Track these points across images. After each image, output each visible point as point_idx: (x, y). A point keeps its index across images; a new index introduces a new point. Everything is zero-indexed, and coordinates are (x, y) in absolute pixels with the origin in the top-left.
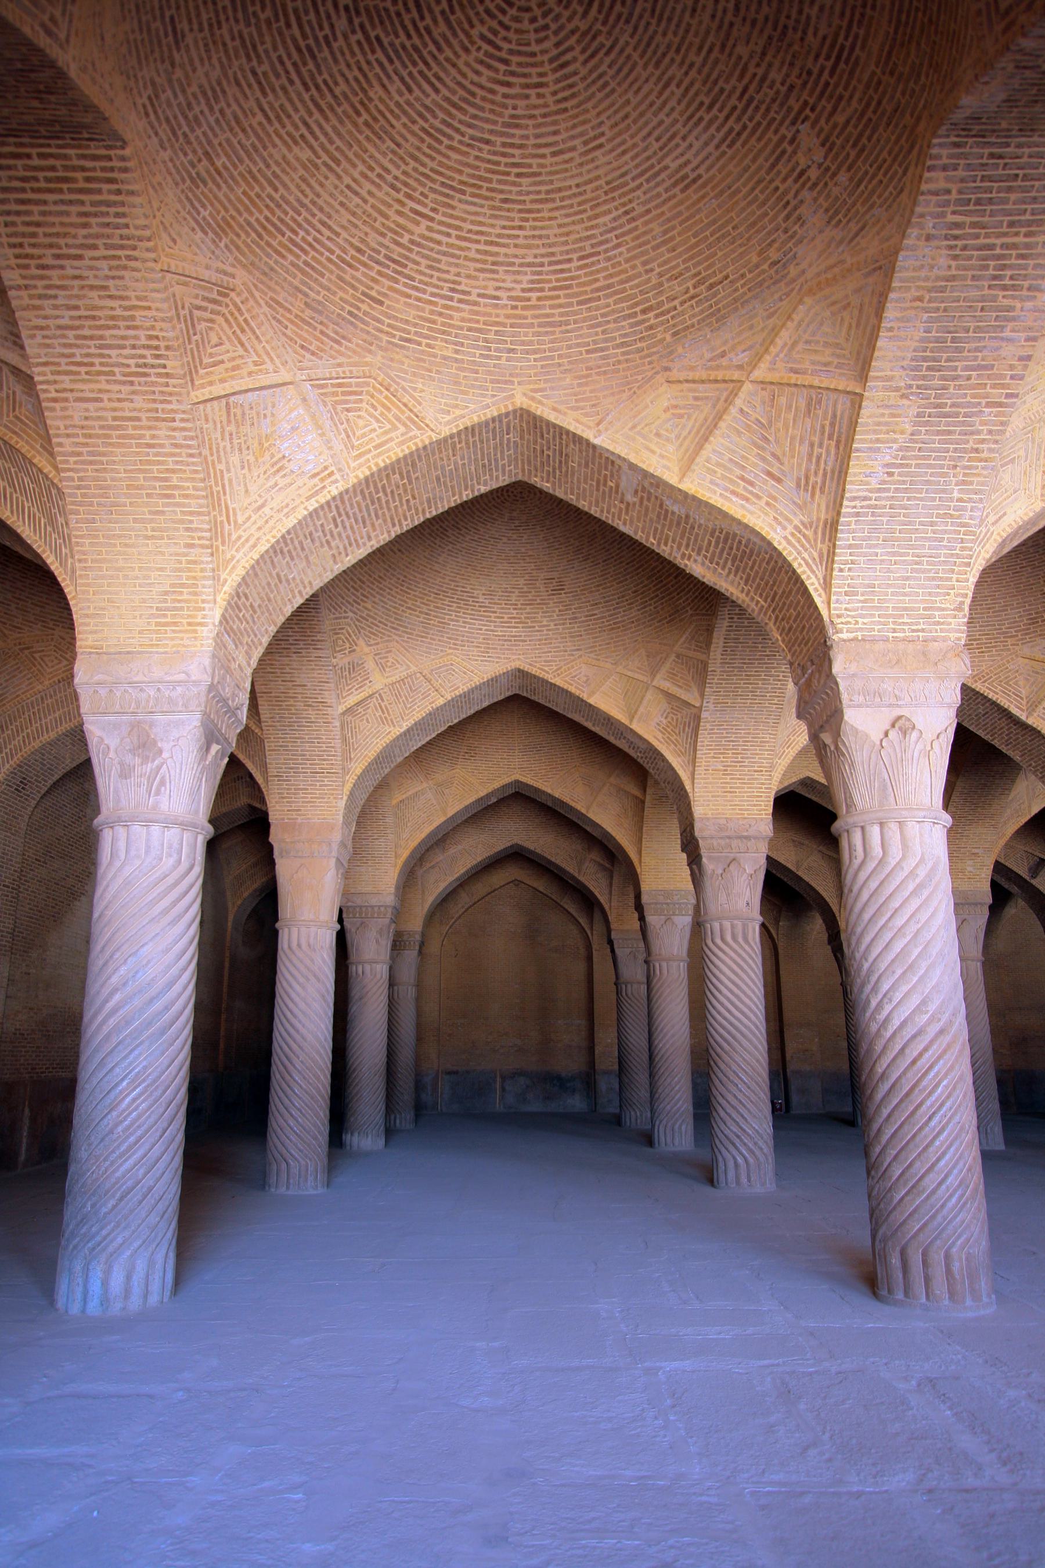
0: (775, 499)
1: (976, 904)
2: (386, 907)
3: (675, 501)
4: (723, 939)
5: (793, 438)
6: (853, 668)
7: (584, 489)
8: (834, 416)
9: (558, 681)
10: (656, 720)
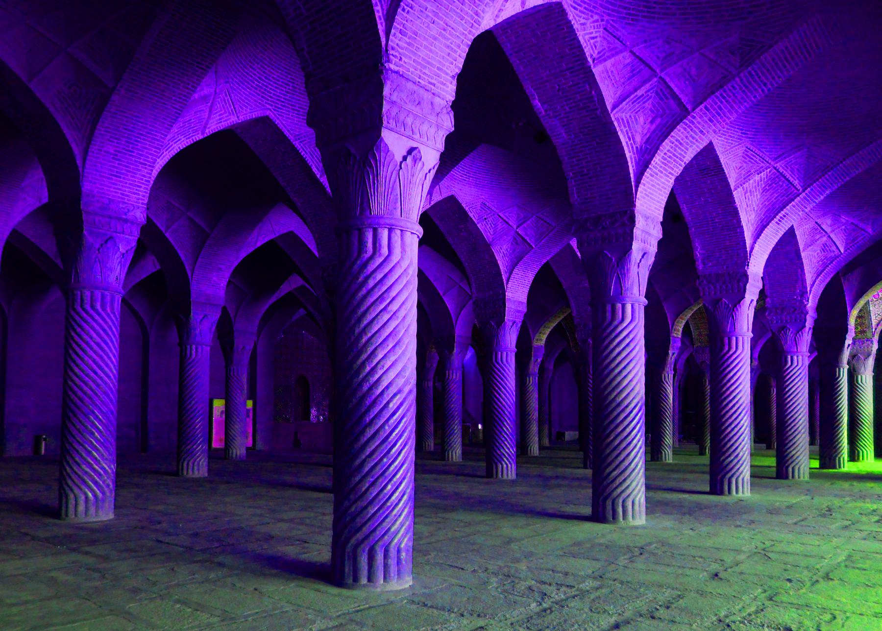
6: (394, 98)
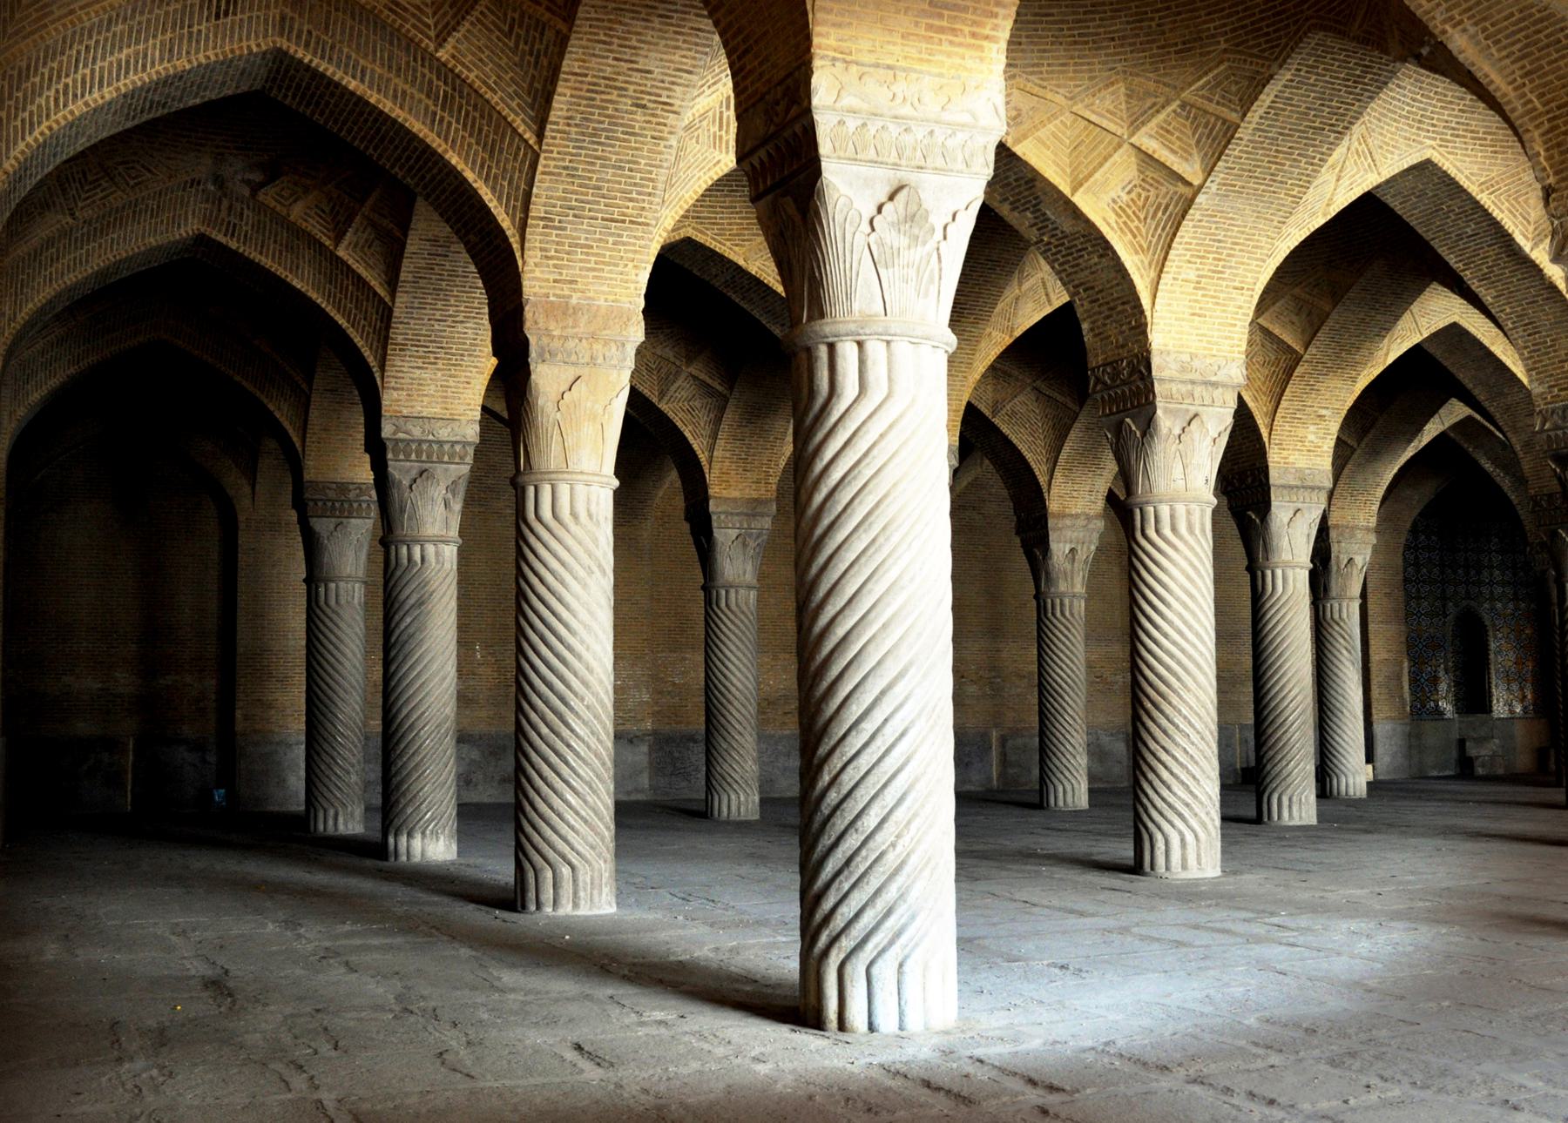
1: (1313, 488)
2: (465, 444)
4: (1174, 529)
10: (1113, 194)
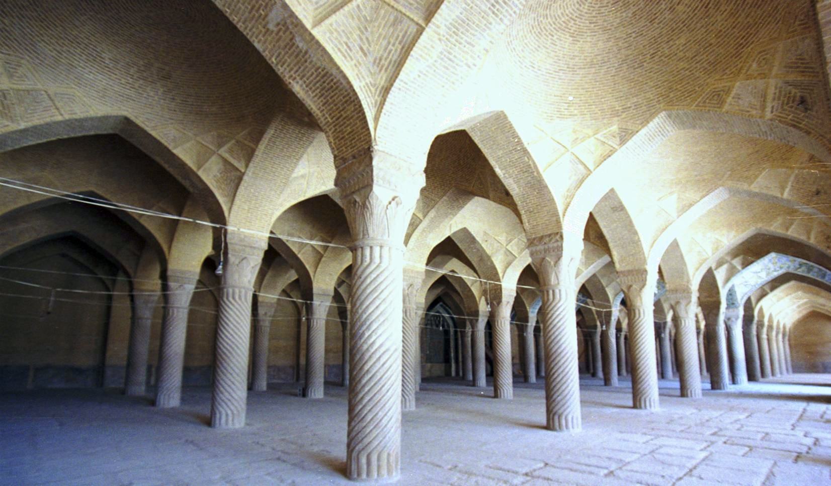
0: (360, 64)
3: (304, 40)
5: (380, 35)
7: (240, 8)
8: (406, 32)
9: (154, 133)
